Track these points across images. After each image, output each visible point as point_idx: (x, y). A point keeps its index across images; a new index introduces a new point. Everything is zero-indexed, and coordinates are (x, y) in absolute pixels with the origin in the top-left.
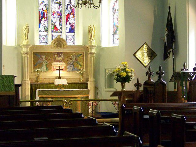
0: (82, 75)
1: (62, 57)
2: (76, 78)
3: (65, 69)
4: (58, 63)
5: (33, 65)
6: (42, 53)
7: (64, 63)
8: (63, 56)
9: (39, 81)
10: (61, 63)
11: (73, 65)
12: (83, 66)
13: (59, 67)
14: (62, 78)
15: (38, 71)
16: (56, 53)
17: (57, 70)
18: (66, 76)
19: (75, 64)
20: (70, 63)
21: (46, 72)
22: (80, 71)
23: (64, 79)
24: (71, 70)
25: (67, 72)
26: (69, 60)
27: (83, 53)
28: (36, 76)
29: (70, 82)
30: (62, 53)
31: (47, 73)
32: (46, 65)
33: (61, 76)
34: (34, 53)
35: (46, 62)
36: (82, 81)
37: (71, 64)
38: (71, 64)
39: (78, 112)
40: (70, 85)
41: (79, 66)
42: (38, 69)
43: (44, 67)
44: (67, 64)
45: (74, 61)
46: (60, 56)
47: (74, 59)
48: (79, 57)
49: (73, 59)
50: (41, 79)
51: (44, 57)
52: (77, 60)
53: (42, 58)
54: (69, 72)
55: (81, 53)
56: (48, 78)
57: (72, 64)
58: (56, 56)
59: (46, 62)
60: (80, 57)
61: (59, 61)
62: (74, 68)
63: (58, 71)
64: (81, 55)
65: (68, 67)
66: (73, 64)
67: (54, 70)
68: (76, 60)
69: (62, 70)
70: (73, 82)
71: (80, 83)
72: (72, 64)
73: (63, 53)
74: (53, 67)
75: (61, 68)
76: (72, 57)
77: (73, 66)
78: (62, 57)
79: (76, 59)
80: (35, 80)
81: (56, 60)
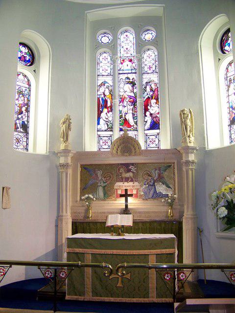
0: (171, 205)
1: (133, 172)
2: (161, 212)
4: (126, 184)
5: (81, 188)
7: (136, 184)
8: (136, 170)
9: (89, 217)
10: (131, 184)
11: (153, 187)
13: (126, 190)
15: (88, 198)
17: (121, 196)
21: (104, 200)
24: (151, 196)
25: (143, 199)
27: (174, 163)
28: (84, 208)
30: (133, 164)
31: (107, 202)
32: (104, 187)
33: (129, 207)
34: (82, 166)
40: (148, 225)
42: (87, 196)
43: (101, 192)
45: (155, 179)
46: (129, 171)
47: (155, 175)
49: (154, 174)
50: (95, 213)
51: (99, 173)
53: (97, 175)
54: (147, 200)
56: (106, 211)
57: (151, 184)
58: (122, 170)
59: (104, 183)
61: (127, 180)
63: (124, 199)
69: (131, 195)
72: (151, 184)
73: (135, 164)
78: (133, 172)
79: (159, 175)
80: (83, 215)
81: (122, 178)
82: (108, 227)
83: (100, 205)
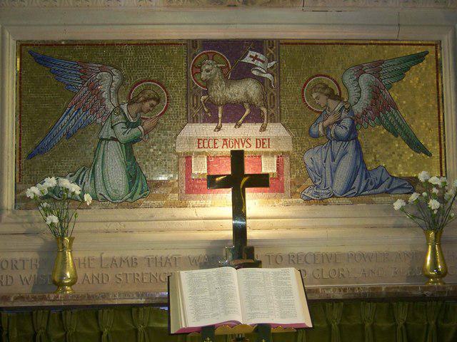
0: (435, 224)
1: (261, 80)
2: (386, 256)
3: (287, 179)
4: (229, 131)
5: (19, 150)
6: (91, 45)
7: (276, 130)
8: (276, 71)
9: (59, 284)
10: (251, 130)
11: (351, 147)
12: (434, 148)
13: (237, 157)
14: (259, 255)
15: (56, 196)
16: (209, 44)
17: (213, 182)
18: (293, 233)
19: (372, 136)
20: (326, 129)
21: (130, 202)
22: (414, 197)
23: (278, 261)
24: (339, 185)
25: (308, 201)
26: (323, 100)
27: (437, 45)
28: (38, 242)
29: (332, 289)
30: (258, 45)
31: (140, 213)
32: (129, 146)
33: (251, 234)
34: (24, 49)
35: (129, 125)
36: (441, 275)
37: (338, 138)
38: (338, 138)
39: (264, 171)
40: (336, 313)
41: (409, 154)
42: (51, 182)
43: (114, 172)
44: (304, 135)
45: (358, 109)
46: (242, 73)
47: (359, 94)
48: (401, 74)
49: (352, 90)
50: (87, 263)
51: (107, 82)
52: (392, 105)
53: (93, 89)
54: (322, 201)
55: (419, 50)
56: (140, 254)
57: (342, 132)
58: (210, 69)
59: (129, 125)
60: (412, 78)
61: (234, 113)
62: (360, 168)
63: (227, 195)
64: (419, 58)
65: (313, 158)
66: (352, 135)
67: (192, 188)
68: (381, 106)
69: (260, 181)
70: (365, 284)
71: (423, 298)
72: (342, 132)
73: (271, 42)
74: (189, 165)
75: (434, 47)
76: (348, 79)
77: (358, 147)
78: (261, 80)
79: (376, 93)
80: (29, 273)
81: (212, 105)
82: (185, 334)
83: (112, 226)
